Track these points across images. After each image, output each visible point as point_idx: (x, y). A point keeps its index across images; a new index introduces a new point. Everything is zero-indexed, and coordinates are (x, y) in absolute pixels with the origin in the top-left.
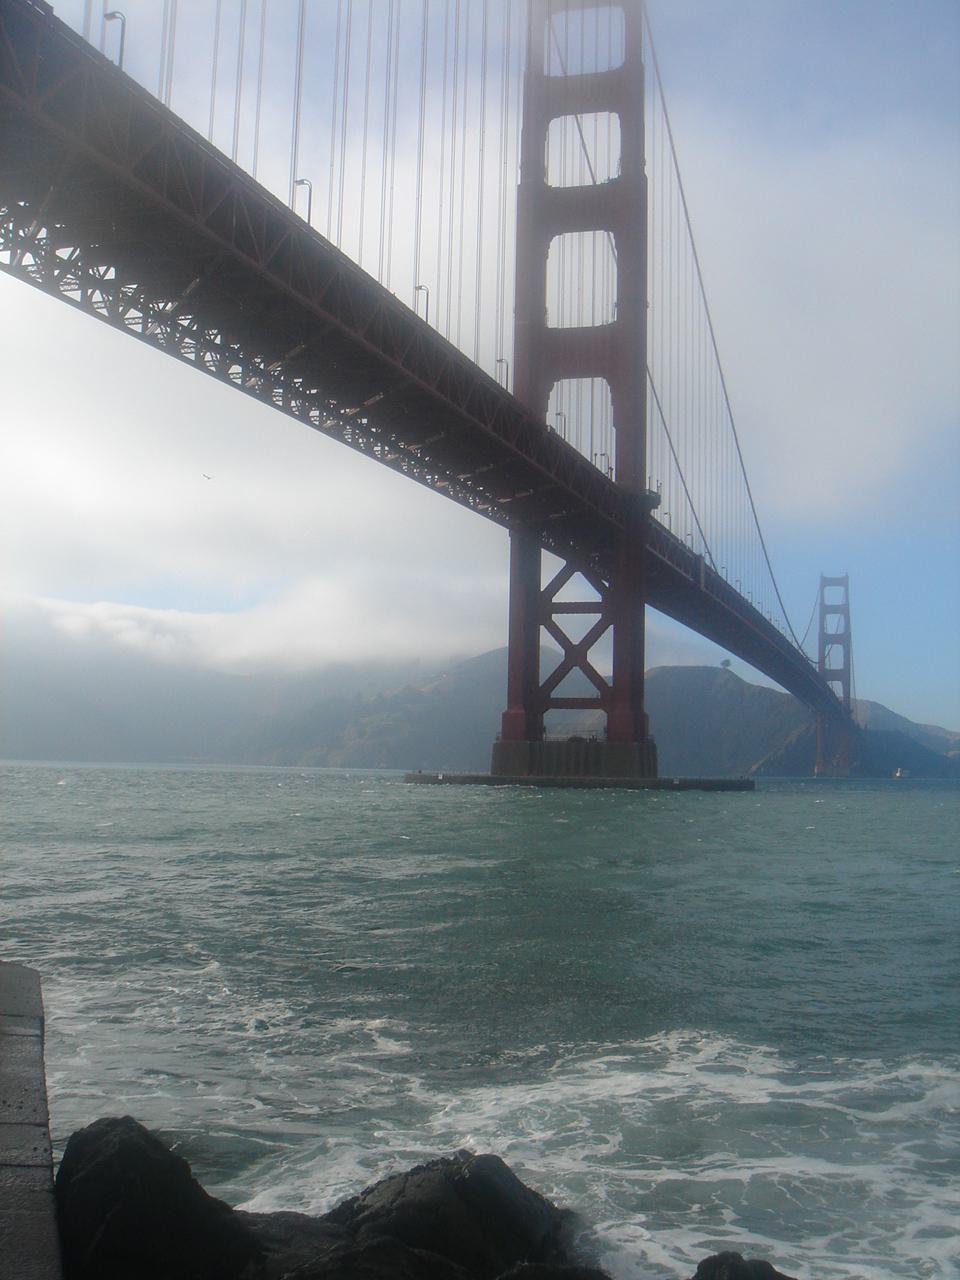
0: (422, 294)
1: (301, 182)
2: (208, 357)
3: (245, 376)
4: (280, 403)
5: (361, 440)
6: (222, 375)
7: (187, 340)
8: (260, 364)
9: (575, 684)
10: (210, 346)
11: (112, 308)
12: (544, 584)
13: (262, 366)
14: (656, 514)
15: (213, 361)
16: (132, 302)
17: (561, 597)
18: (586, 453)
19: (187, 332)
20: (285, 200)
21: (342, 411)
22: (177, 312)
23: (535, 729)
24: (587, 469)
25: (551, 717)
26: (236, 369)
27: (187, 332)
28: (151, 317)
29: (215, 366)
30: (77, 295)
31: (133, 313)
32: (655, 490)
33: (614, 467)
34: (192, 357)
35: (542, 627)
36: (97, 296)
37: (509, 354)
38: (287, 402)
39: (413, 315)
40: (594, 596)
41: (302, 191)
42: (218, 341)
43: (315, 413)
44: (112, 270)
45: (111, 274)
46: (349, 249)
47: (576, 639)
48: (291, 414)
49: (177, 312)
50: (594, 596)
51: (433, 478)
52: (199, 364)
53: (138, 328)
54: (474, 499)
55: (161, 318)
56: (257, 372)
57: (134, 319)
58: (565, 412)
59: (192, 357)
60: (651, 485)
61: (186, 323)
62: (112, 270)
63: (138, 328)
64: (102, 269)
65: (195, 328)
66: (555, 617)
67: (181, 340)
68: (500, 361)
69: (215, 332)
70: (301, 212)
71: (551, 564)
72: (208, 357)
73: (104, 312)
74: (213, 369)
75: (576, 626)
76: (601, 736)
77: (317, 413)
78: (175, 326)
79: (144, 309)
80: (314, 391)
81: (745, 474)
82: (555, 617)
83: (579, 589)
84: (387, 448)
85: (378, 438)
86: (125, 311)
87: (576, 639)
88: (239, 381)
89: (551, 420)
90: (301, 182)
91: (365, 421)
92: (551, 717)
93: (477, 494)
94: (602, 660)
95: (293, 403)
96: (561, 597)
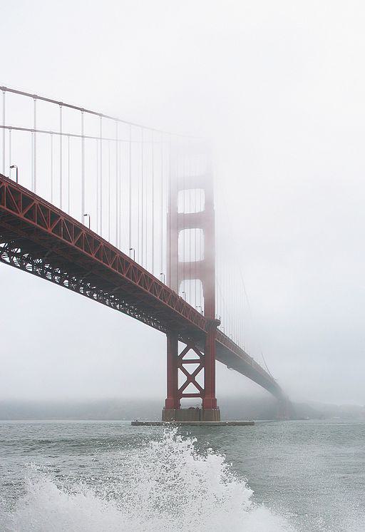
2: (56, 278)
6: (61, 284)
9: (191, 389)
10: (57, 274)
11: (21, 262)
16: (28, 260)
19: (48, 270)
22: (44, 263)
23: (177, 405)
24: (194, 311)
25: (183, 400)
26: (66, 281)
27: (48, 270)
30: (7, 259)
31: (29, 265)
36: (15, 259)
37: (165, 272)
38: (84, 290)
41: (86, 218)
43: (95, 295)
44: (19, 250)
45: (19, 251)
46: (105, 236)
48: (86, 295)
49: (44, 263)
52: (53, 280)
53: (31, 270)
55: (38, 265)
56: (74, 282)
62: (19, 250)
64: (16, 250)
71: (182, 346)
72: (56, 278)
75: (191, 368)
76: (200, 407)
78: (44, 268)
79: (33, 263)
83: (192, 355)
86: (26, 265)
92: (183, 400)
93: (154, 321)
94: (200, 378)
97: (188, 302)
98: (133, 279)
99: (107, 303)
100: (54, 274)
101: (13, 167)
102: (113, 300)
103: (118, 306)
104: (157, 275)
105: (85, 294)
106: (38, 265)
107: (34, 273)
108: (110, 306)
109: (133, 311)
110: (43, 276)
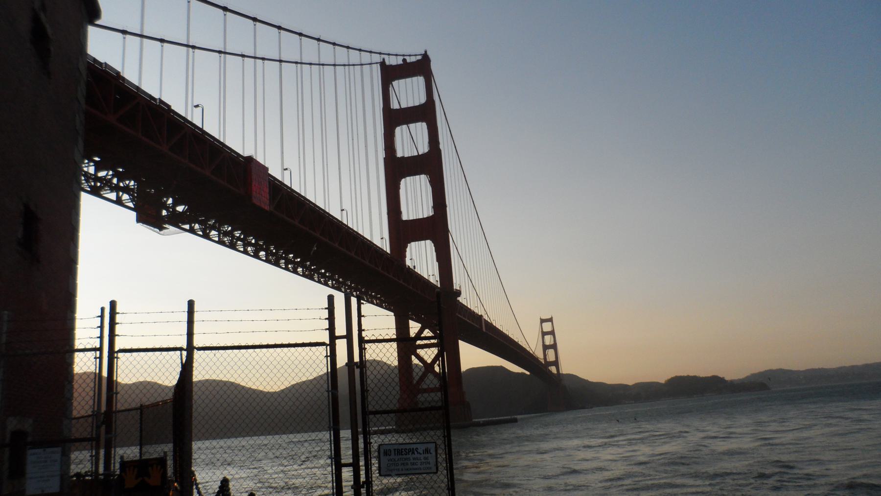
0: (344, 212)
1: (286, 169)
2: (249, 249)
3: (267, 256)
4: (284, 267)
6: (256, 256)
7: (239, 242)
8: (273, 250)
10: (250, 244)
11: (204, 231)
13: (274, 251)
15: (252, 250)
16: (213, 228)
18: (426, 276)
19: (239, 239)
20: (280, 178)
21: (313, 268)
26: (262, 253)
28: (222, 234)
29: (253, 252)
31: (213, 233)
34: (242, 249)
37: (386, 235)
38: (286, 264)
41: (287, 173)
42: (253, 241)
43: (300, 270)
46: (310, 197)
49: (233, 230)
51: (356, 293)
52: (245, 252)
53: (217, 239)
54: (376, 301)
55: (226, 234)
56: (273, 254)
57: (214, 235)
58: (414, 257)
59: (242, 249)
61: (238, 235)
63: (217, 239)
65: (242, 237)
67: (236, 242)
69: (252, 238)
70: (287, 182)
73: (201, 233)
74: (252, 254)
77: (301, 269)
78: (233, 236)
79: (219, 231)
80: (299, 260)
81: (493, 261)
84: (334, 282)
85: (330, 278)
86: (210, 232)
88: (264, 258)
89: (408, 263)
90: (286, 169)
91: (323, 271)
93: (377, 299)
95: (290, 266)
99: (316, 279)
100: (246, 244)
102: (323, 275)
103: (330, 283)
104: (377, 242)
105: (287, 269)
106: (226, 234)
107: (221, 242)
108: (319, 282)
110: (232, 246)
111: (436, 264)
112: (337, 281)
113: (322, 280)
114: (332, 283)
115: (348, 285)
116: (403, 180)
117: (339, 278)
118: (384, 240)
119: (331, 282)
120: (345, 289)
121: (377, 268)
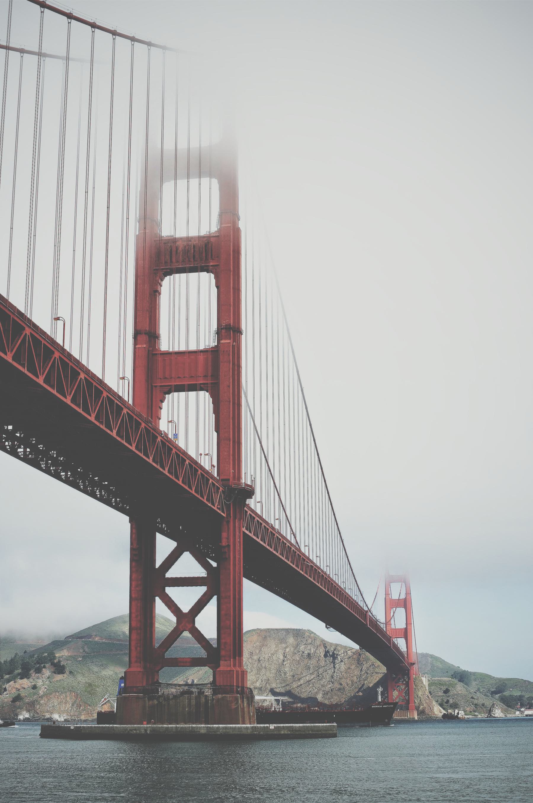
5: (7, 443)
12: (159, 561)
14: (251, 502)
17: (172, 573)
18: (192, 453)
32: (249, 483)
33: (215, 463)
35: (157, 598)
37: (129, 374)
39: (53, 342)
40: (200, 572)
47: (185, 608)
50: (200, 572)
51: (66, 475)
54: (100, 491)
58: (175, 419)
60: (246, 479)
66: (170, 591)
68: (123, 378)
82: (170, 591)
84: (28, 450)
85: (23, 442)
87: (185, 608)
89: (163, 426)
91: (10, 427)
93: (102, 487)
96: (172, 573)
97: (181, 444)
98: (61, 391)
101: (58, 319)
109: (55, 462)
111: (215, 434)
112: (34, 449)
113: (7, 443)
114: (25, 451)
115: (51, 458)
116: (167, 278)
117: (38, 443)
118: (126, 382)
119: (22, 450)
120: (47, 464)
121: (109, 432)
